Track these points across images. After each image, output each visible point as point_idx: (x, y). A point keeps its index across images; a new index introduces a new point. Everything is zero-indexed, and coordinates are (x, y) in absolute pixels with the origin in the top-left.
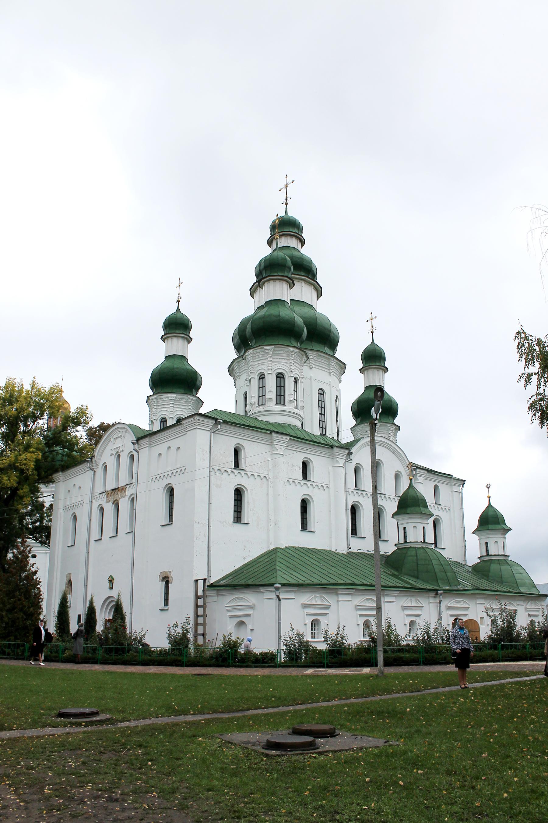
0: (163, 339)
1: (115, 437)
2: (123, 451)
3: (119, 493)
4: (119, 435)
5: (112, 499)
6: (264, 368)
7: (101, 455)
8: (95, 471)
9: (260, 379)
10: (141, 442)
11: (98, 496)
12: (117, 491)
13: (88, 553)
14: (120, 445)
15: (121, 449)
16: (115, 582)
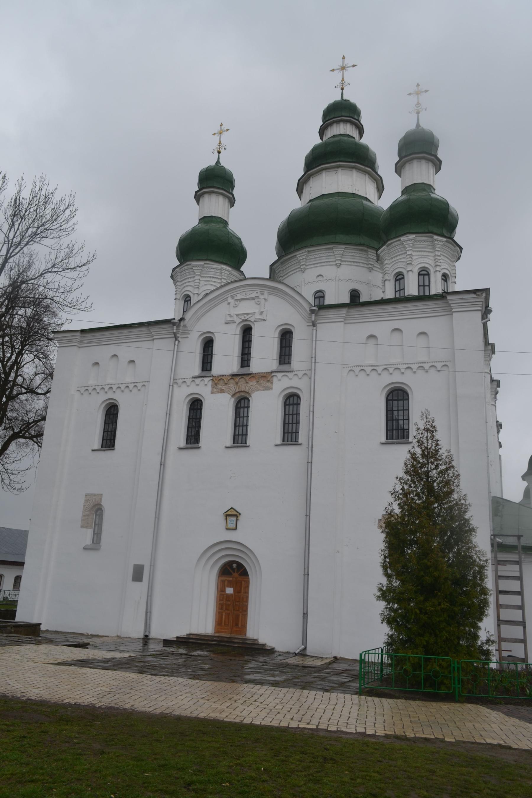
0: (198, 197)
1: (239, 297)
2: (264, 320)
3: (254, 382)
4: (254, 295)
5: (232, 387)
6: (428, 262)
7: (199, 319)
8: (179, 342)
9: (419, 274)
10: (323, 312)
11: (188, 381)
12: (247, 378)
13: (163, 464)
14: (256, 311)
15: (258, 317)
16: (240, 518)
